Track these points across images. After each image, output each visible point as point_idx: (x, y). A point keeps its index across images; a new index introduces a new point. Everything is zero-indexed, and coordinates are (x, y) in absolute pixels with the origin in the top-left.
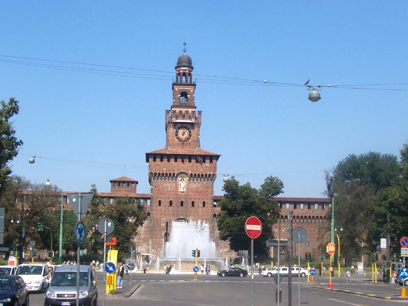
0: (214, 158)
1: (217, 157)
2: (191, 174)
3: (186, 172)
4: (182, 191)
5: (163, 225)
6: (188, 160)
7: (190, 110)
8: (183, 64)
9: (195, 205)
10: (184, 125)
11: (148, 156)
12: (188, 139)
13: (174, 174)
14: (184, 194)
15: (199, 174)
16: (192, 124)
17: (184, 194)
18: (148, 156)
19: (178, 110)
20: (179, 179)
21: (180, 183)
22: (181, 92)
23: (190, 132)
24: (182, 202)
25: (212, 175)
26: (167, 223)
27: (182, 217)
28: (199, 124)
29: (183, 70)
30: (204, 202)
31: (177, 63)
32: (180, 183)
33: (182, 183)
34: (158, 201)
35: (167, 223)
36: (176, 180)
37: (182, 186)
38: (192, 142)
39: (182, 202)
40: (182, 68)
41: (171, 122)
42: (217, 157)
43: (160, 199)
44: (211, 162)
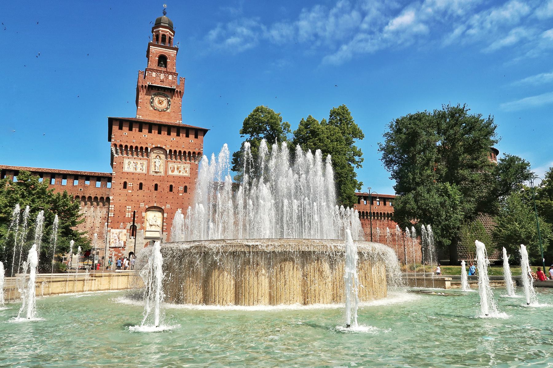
0: (199, 132)
1: (204, 132)
2: (170, 151)
3: (164, 147)
4: (157, 170)
5: (129, 215)
6: (166, 133)
7: (170, 77)
8: (162, 24)
9: (174, 189)
10: (163, 92)
11: (111, 121)
12: (167, 109)
13: (147, 148)
14: (158, 174)
15: (180, 152)
16: (172, 91)
17: (158, 174)
18: (111, 121)
19: (154, 74)
20: (153, 155)
21: (154, 160)
22: (160, 54)
23: (169, 101)
24: (156, 186)
25: (197, 153)
26: (134, 212)
27: (155, 205)
28: (180, 94)
29: (162, 31)
30: (186, 188)
31: (155, 24)
32: (154, 160)
33: (157, 160)
34: (122, 182)
35: (134, 212)
36: (147, 156)
37: (157, 164)
38: (172, 114)
39: (156, 186)
40: (161, 29)
41: (146, 86)
42: (204, 132)
43: (126, 180)
44: (196, 137)
